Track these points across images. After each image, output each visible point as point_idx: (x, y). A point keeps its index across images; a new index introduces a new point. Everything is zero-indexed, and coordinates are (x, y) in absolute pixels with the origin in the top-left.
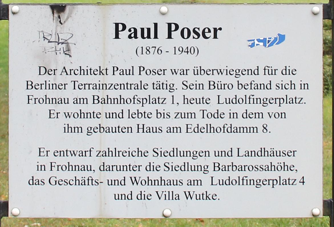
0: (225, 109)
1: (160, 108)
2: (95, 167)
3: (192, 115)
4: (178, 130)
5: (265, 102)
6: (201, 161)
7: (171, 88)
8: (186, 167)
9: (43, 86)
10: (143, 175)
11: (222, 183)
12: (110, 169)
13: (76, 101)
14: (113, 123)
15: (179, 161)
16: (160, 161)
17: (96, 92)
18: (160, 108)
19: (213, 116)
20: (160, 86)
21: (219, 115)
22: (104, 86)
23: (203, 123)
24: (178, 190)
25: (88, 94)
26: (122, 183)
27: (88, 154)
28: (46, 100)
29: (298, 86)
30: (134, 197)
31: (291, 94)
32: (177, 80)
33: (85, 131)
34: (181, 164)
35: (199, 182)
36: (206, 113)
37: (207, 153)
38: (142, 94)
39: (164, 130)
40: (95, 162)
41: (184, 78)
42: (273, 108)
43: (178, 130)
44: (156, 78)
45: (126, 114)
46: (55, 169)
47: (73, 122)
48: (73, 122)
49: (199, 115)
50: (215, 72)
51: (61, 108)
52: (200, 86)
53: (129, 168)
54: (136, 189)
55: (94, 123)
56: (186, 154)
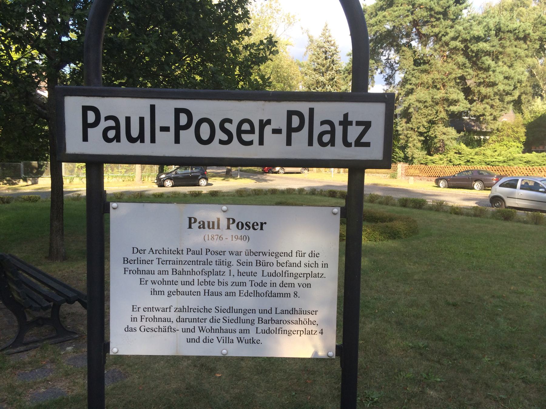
0: (267, 280)
1: (221, 278)
2: (173, 319)
3: (244, 284)
4: (233, 294)
5: (296, 276)
6: (250, 316)
7: (229, 265)
8: (238, 320)
9: (136, 262)
10: (208, 325)
11: (264, 332)
12: (184, 320)
13: (160, 273)
14: (187, 288)
15: (233, 316)
16: (220, 316)
17: (174, 267)
18: (221, 278)
19: (258, 284)
20: (220, 263)
21: (263, 284)
22: (180, 262)
23: (251, 290)
24: (233, 336)
25: (169, 267)
26: (193, 331)
27: (168, 310)
28: (138, 271)
29: (320, 266)
30: (201, 340)
31: (315, 271)
32: (233, 259)
33: (166, 294)
34: (235, 318)
35: (247, 331)
36: (253, 283)
37: (254, 311)
38: (208, 268)
39: (224, 294)
40: (173, 315)
41: (238, 257)
42: (301, 280)
43: (233, 294)
44: (218, 257)
45: (196, 282)
46: (144, 320)
47: (158, 288)
48: (158, 288)
49: (249, 284)
50: (261, 254)
51: (150, 277)
52: (250, 264)
53: (198, 320)
54: (203, 335)
55: (173, 288)
56: (238, 311)
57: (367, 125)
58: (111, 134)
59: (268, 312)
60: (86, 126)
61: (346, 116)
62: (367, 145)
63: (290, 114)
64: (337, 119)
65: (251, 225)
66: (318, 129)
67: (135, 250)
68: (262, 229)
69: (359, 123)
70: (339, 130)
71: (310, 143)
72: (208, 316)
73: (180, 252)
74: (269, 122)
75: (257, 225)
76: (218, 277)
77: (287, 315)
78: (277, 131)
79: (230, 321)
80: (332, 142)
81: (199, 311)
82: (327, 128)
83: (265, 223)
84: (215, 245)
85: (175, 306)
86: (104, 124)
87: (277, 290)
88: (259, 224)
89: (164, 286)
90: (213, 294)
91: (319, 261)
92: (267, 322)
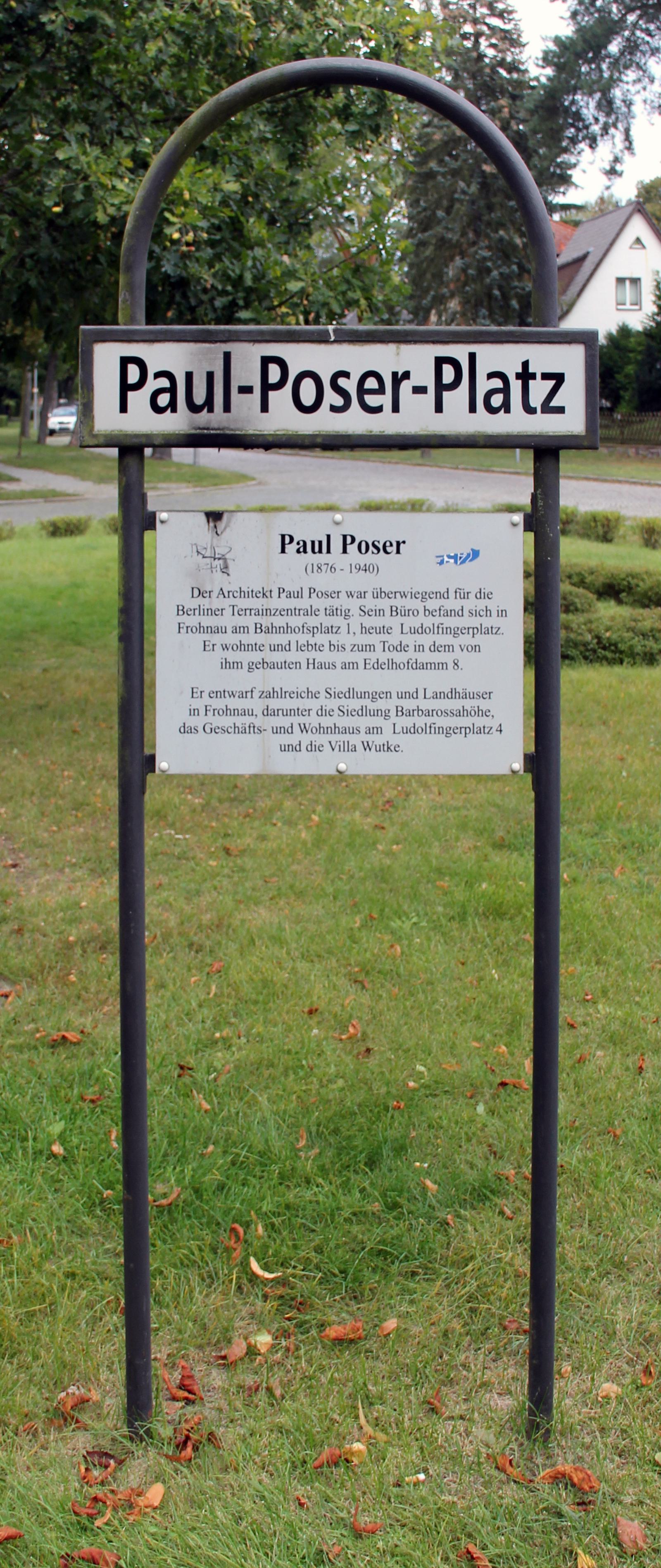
0: (410, 640)
1: (334, 638)
2: (258, 711)
3: (371, 647)
4: (353, 665)
5: (456, 632)
6: (381, 704)
7: (347, 615)
8: (363, 712)
9: (197, 612)
10: (313, 720)
11: (407, 731)
12: (275, 713)
13: (235, 630)
14: (278, 657)
15: (355, 704)
16: (333, 704)
17: (258, 619)
18: (334, 638)
19: (395, 648)
20: (333, 612)
21: (402, 648)
22: (267, 612)
23: (384, 657)
24: (355, 740)
25: (249, 621)
26: (289, 731)
27: (249, 695)
28: (200, 629)
29: (494, 613)
30: (303, 748)
31: (487, 622)
32: (354, 604)
33: (245, 666)
34: (358, 708)
35: (379, 730)
36: (387, 645)
37: (388, 694)
38: (312, 621)
39: (339, 665)
40: (256, 704)
41: (361, 602)
42: (466, 639)
43: (353, 665)
44: (328, 602)
45: (293, 646)
46: (210, 714)
47: (232, 656)
48: (232, 656)
49: (379, 647)
50: (398, 595)
51: (218, 639)
52: (380, 612)
53: (298, 712)
54: (306, 739)
55: (256, 656)
56: (363, 695)
57: (559, 379)
58: (163, 400)
59: (411, 696)
60: (125, 388)
61: (525, 364)
62: (561, 410)
63: (440, 362)
64: (512, 369)
65: (381, 546)
66: (483, 385)
67: (196, 592)
68: (398, 552)
69: (546, 376)
70: (516, 386)
71: (473, 409)
72: (313, 704)
73: (268, 594)
74: (407, 375)
75: (391, 545)
76: (330, 637)
77: (453, 618)
78: (419, 390)
79: (350, 713)
80: (506, 406)
81: (299, 696)
82: (498, 383)
83: (404, 542)
84: (323, 581)
85: (260, 688)
86: (152, 385)
87: (425, 657)
88: (395, 544)
89: (243, 653)
90: (322, 666)
91: (492, 605)
92: (410, 713)
